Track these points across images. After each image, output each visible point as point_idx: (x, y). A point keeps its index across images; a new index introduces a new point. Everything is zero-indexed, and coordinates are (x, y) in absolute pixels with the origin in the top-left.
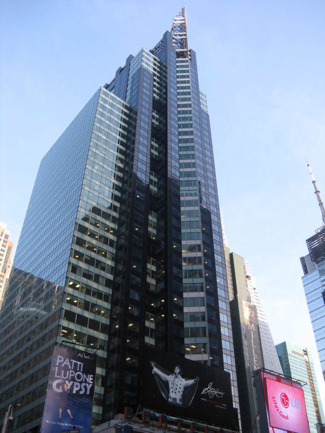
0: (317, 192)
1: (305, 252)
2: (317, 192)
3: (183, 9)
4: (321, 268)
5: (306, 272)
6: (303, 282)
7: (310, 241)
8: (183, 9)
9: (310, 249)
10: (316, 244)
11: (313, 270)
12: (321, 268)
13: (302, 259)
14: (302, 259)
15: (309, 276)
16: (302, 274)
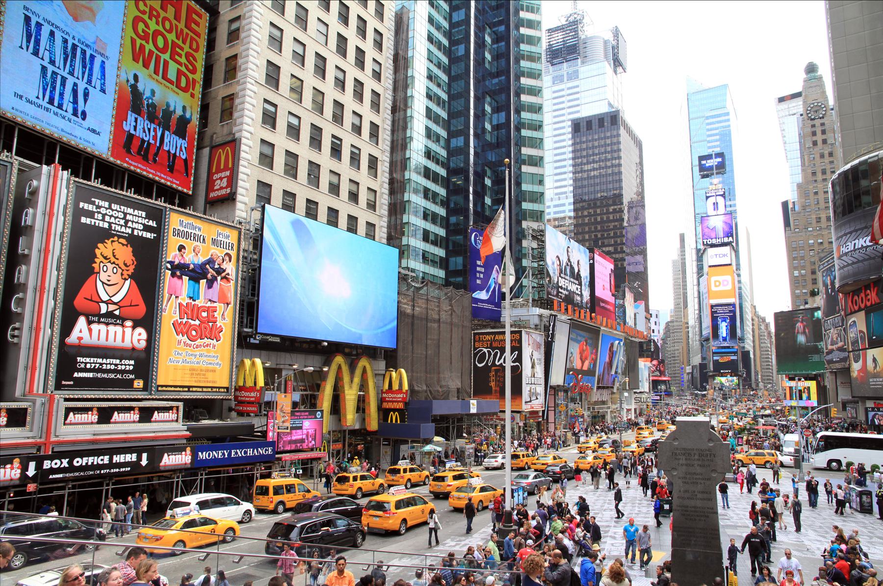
4: (556, 74)
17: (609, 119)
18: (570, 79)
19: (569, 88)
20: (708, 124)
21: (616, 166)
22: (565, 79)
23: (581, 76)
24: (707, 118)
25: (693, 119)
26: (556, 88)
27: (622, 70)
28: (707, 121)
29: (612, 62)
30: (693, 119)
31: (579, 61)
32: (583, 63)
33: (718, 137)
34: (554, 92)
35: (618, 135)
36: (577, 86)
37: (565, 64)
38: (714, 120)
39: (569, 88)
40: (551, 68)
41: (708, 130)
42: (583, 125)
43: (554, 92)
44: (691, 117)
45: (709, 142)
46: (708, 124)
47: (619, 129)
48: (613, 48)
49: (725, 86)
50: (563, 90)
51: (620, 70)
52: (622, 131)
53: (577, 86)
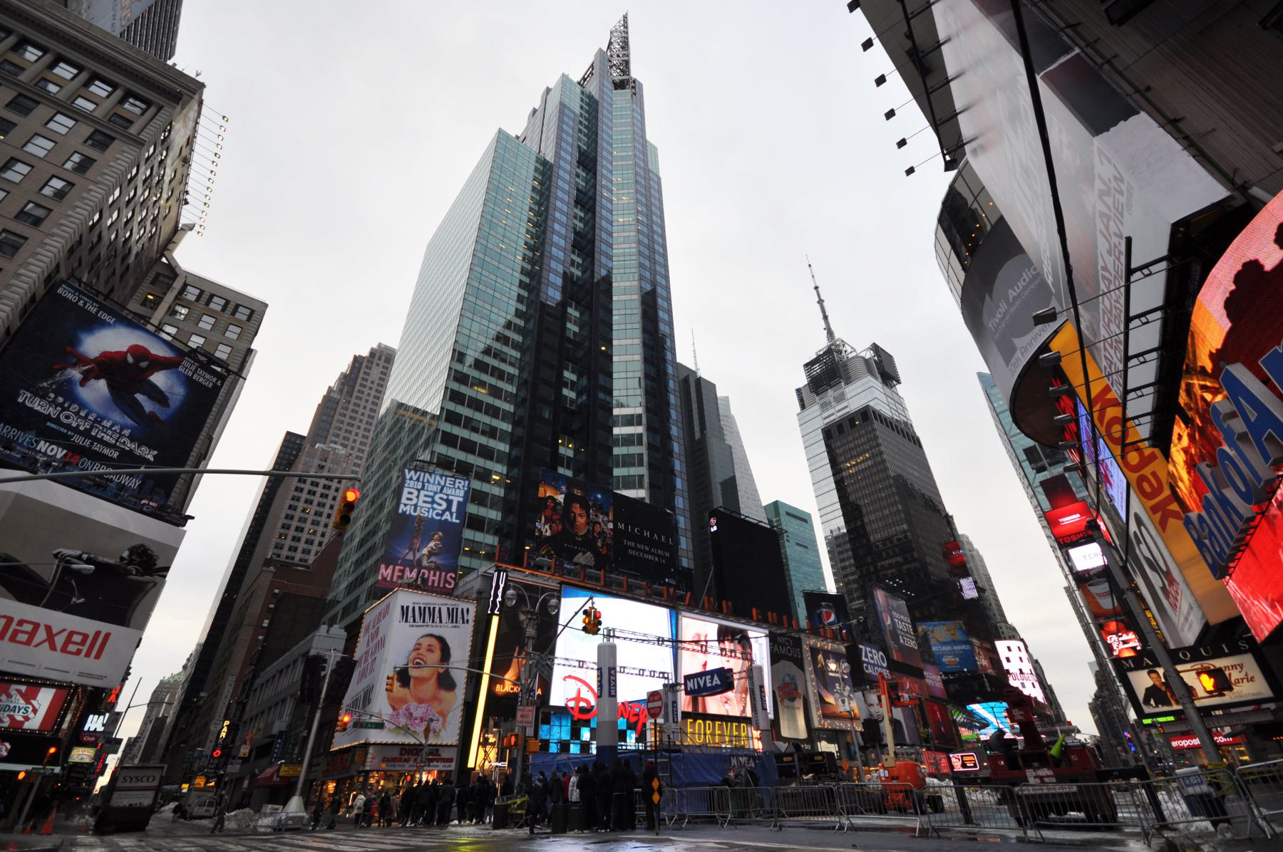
0: (821, 302)
1: (802, 381)
2: (821, 302)
3: (625, 17)
4: (823, 401)
5: (803, 407)
6: (799, 420)
7: (808, 366)
8: (625, 17)
9: (809, 376)
10: (817, 369)
12: (823, 401)
13: (798, 391)
14: (798, 391)
15: (806, 412)
16: (798, 409)
17: (860, 416)
19: (839, 411)
21: (879, 463)
22: (833, 404)
23: (848, 396)
25: (1001, 413)
26: (824, 415)
29: (879, 376)
30: (1001, 413)
32: (847, 383)
35: (874, 430)
36: (846, 407)
39: (839, 411)
40: (817, 398)
42: (835, 431)
44: (998, 410)
47: (872, 423)
53: (846, 407)
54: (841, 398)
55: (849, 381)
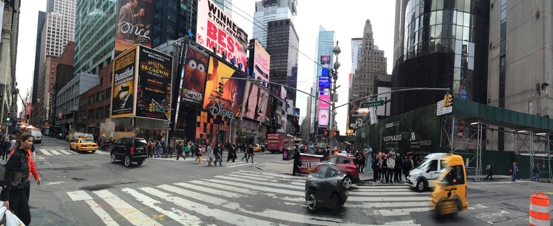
5: (256, 10)
11: (262, 10)
15: (258, 13)
18: (272, 13)
20: (326, 44)
22: (270, 13)
23: (277, 12)
24: (326, 42)
27: (295, 14)
28: (325, 43)
31: (277, 6)
33: (329, 50)
34: (265, 18)
35: (289, 30)
36: (275, 16)
37: (270, 7)
38: (328, 43)
39: (271, 17)
41: (325, 47)
43: (265, 18)
45: (325, 51)
46: (326, 44)
48: (292, 3)
49: (334, 32)
50: (268, 18)
51: (294, 14)
52: (291, 27)
54: (274, 12)
55: (279, 6)
